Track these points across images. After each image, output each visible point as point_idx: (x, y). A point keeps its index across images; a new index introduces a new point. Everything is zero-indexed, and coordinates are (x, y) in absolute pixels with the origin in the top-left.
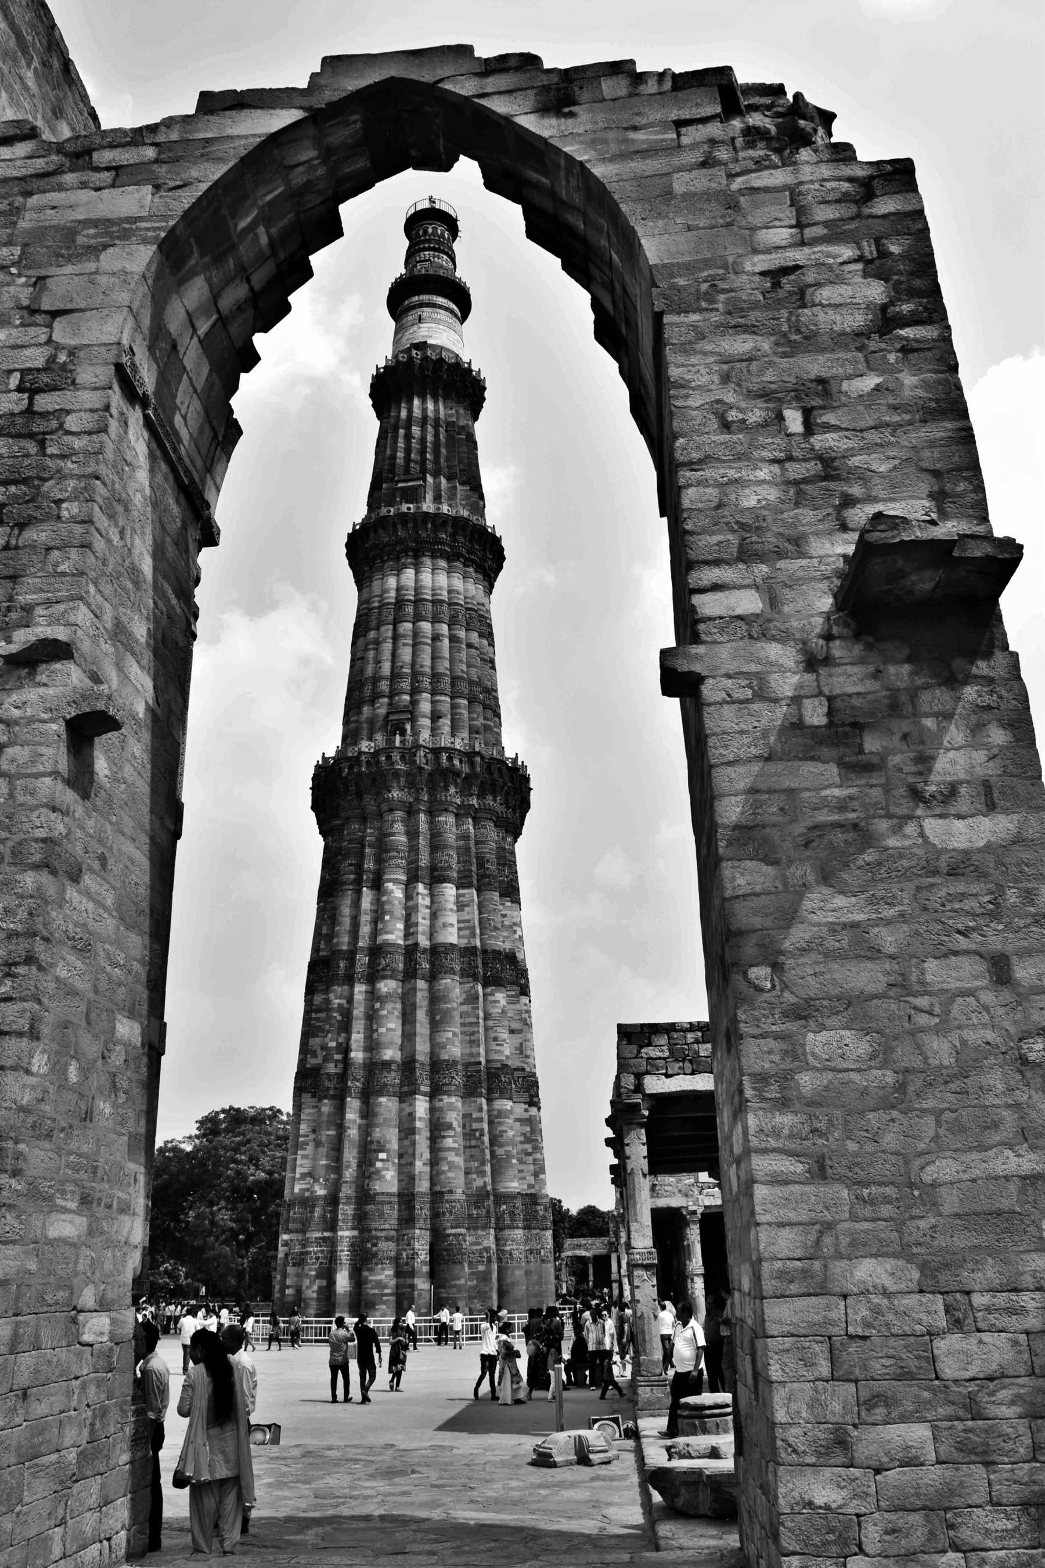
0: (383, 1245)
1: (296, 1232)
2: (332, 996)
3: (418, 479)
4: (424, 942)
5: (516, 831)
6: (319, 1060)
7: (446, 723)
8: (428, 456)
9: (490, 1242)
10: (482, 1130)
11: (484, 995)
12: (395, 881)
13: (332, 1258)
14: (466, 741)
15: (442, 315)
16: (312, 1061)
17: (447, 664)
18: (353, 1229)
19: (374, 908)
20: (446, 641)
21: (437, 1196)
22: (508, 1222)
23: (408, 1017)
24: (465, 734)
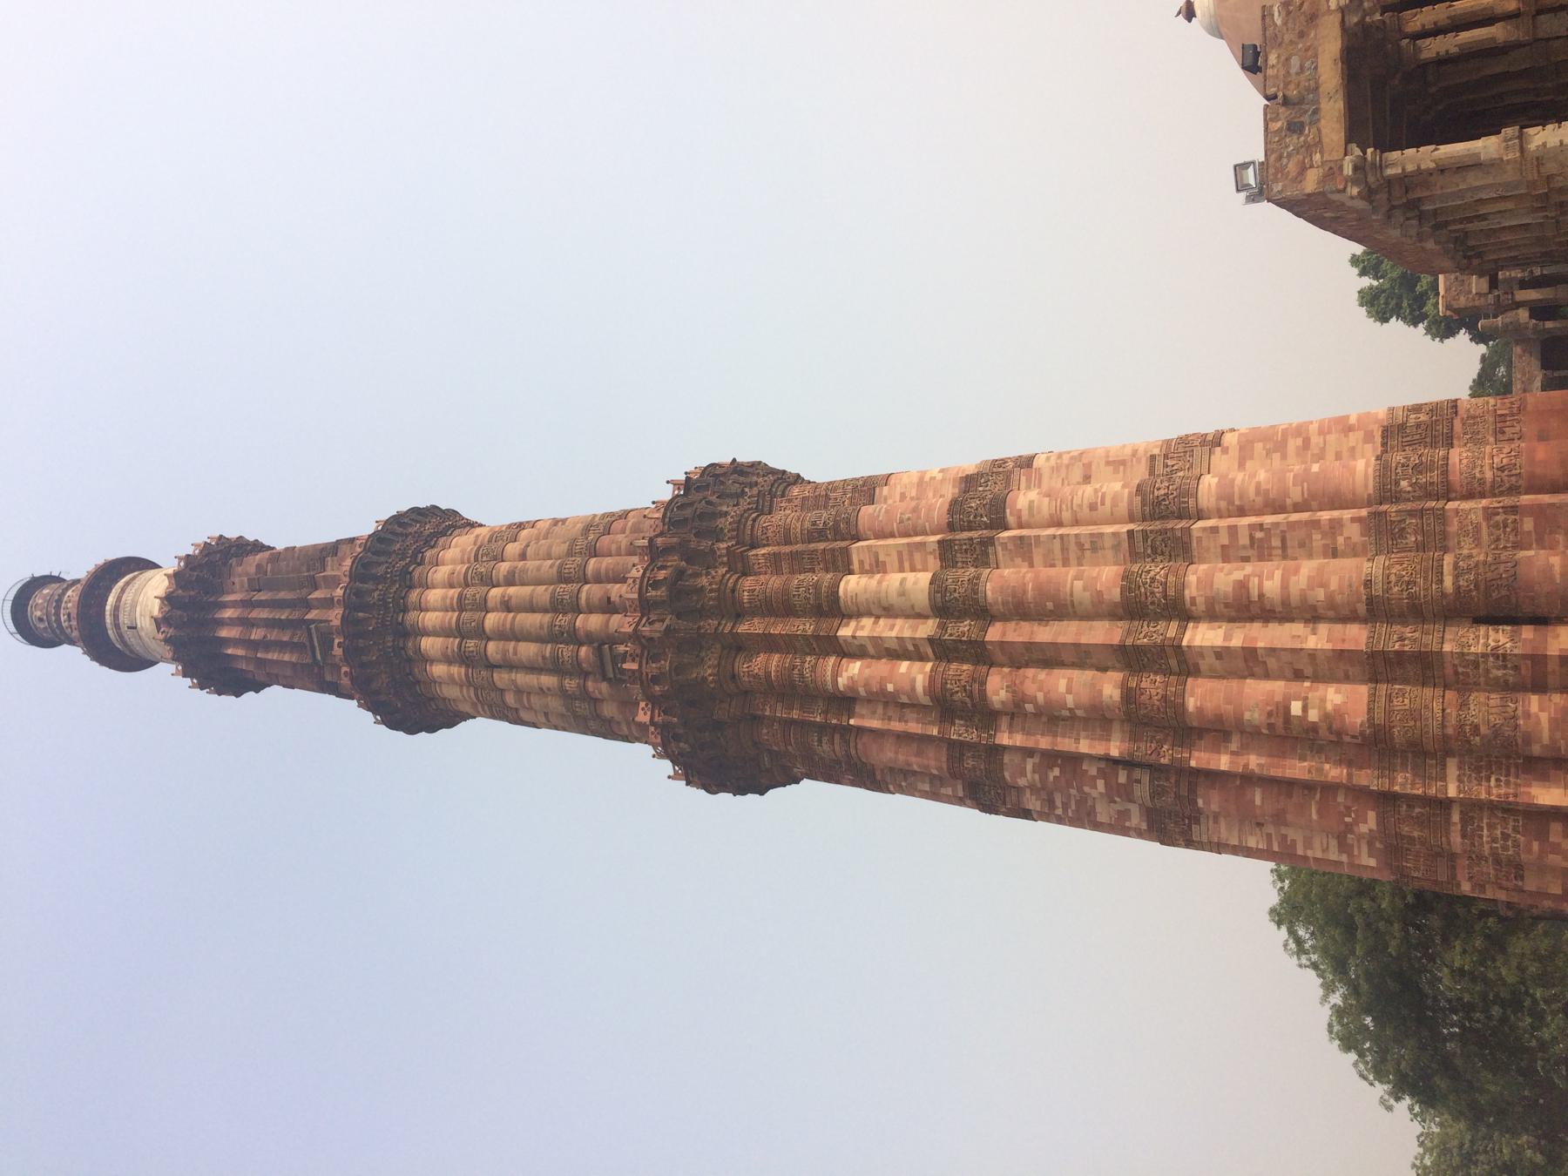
1: (1454, 868)
2: (1022, 782)
3: (309, 630)
5: (785, 480)
6: (1134, 809)
7: (616, 590)
10: (1251, 527)
11: (1020, 526)
12: (836, 675)
13: (1506, 809)
15: (128, 597)
16: (1136, 819)
18: (1444, 767)
19: (880, 710)
20: (512, 590)
21: (1375, 609)
22: (1435, 476)
23: (1050, 657)
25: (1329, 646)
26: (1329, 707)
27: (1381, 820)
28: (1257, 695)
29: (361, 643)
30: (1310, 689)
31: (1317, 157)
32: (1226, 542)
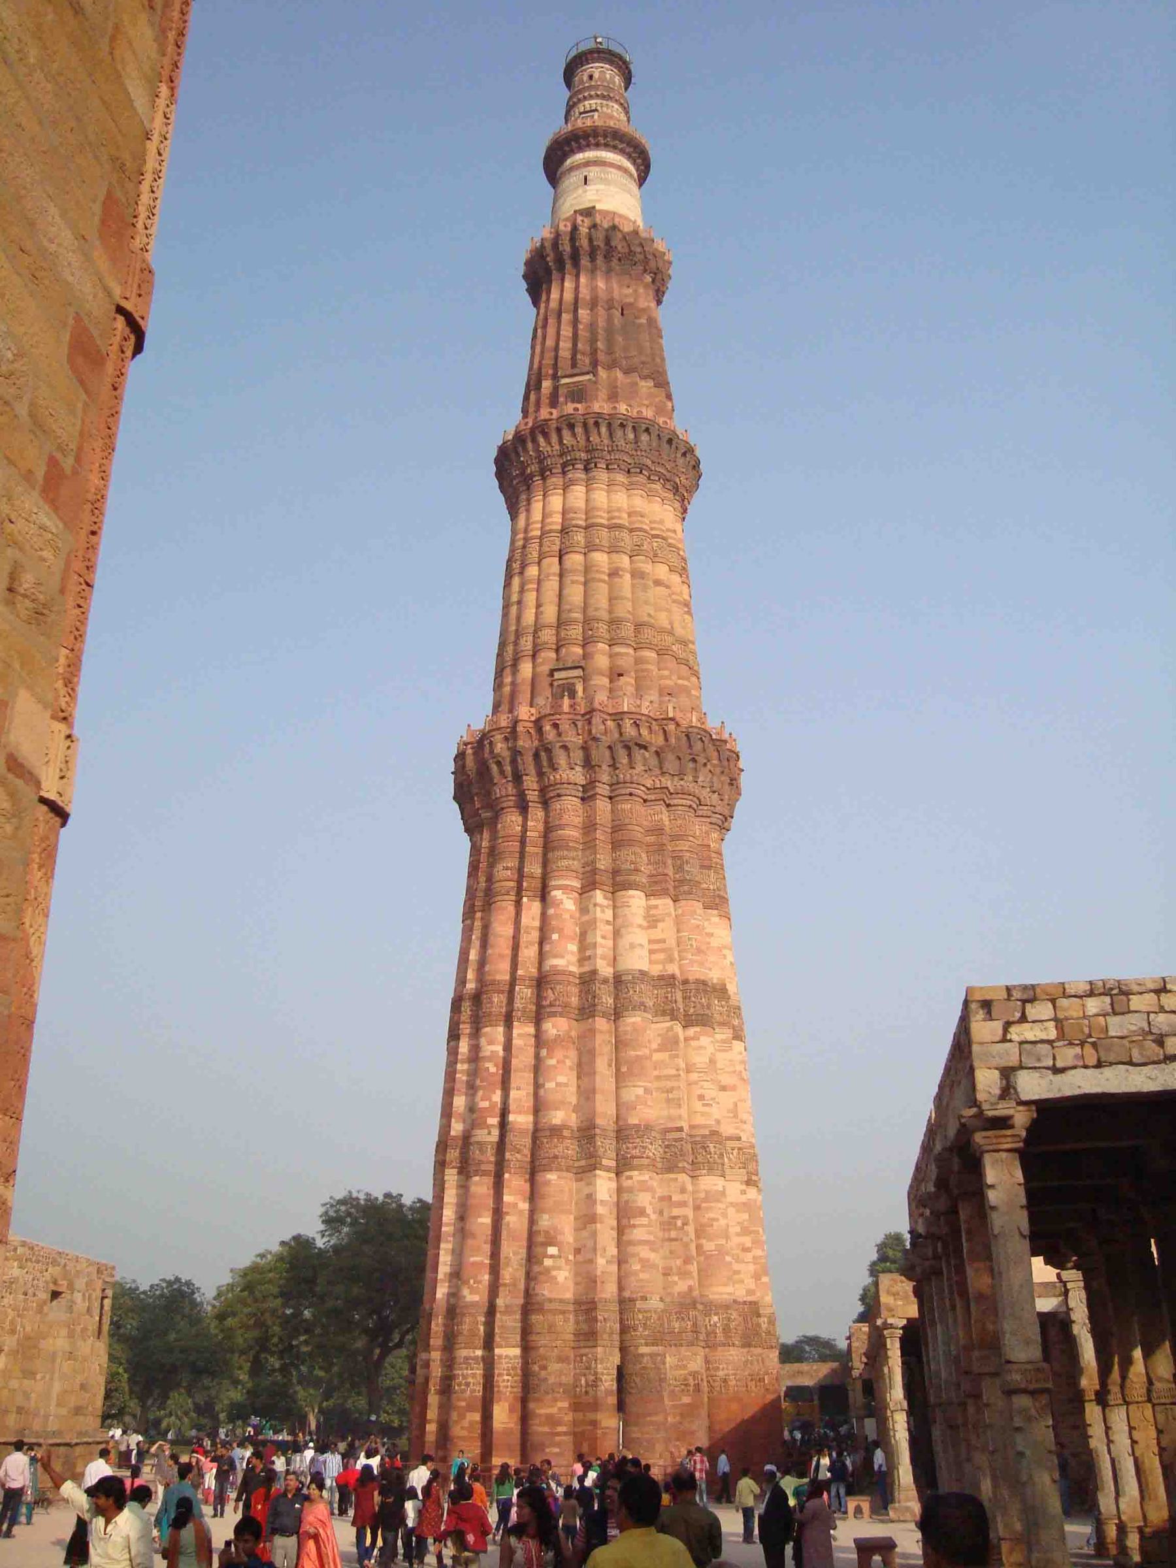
0: (554, 1367)
3: (588, 373)
4: (605, 970)
5: (723, 824)
7: (628, 682)
8: (600, 345)
9: (696, 1364)
10: (686, 1217)
11: (686, 1039)
14: (656, 705)
15: (614, 174)
16: (457, 1128)
17: (629, 605)
19: (537, 924)
20: (628, 576)
21: (625, 1304)
22: (720, 1337)
23: (585, 1069)
24: (653, 696)
25: (599, 1273)
26: (554, 1273)
27: (474, 1304)
28: (561, 1223)
29: (579, 430)
30: (567, 1260)
31: (900, 1303)
32: (674, 1199)
